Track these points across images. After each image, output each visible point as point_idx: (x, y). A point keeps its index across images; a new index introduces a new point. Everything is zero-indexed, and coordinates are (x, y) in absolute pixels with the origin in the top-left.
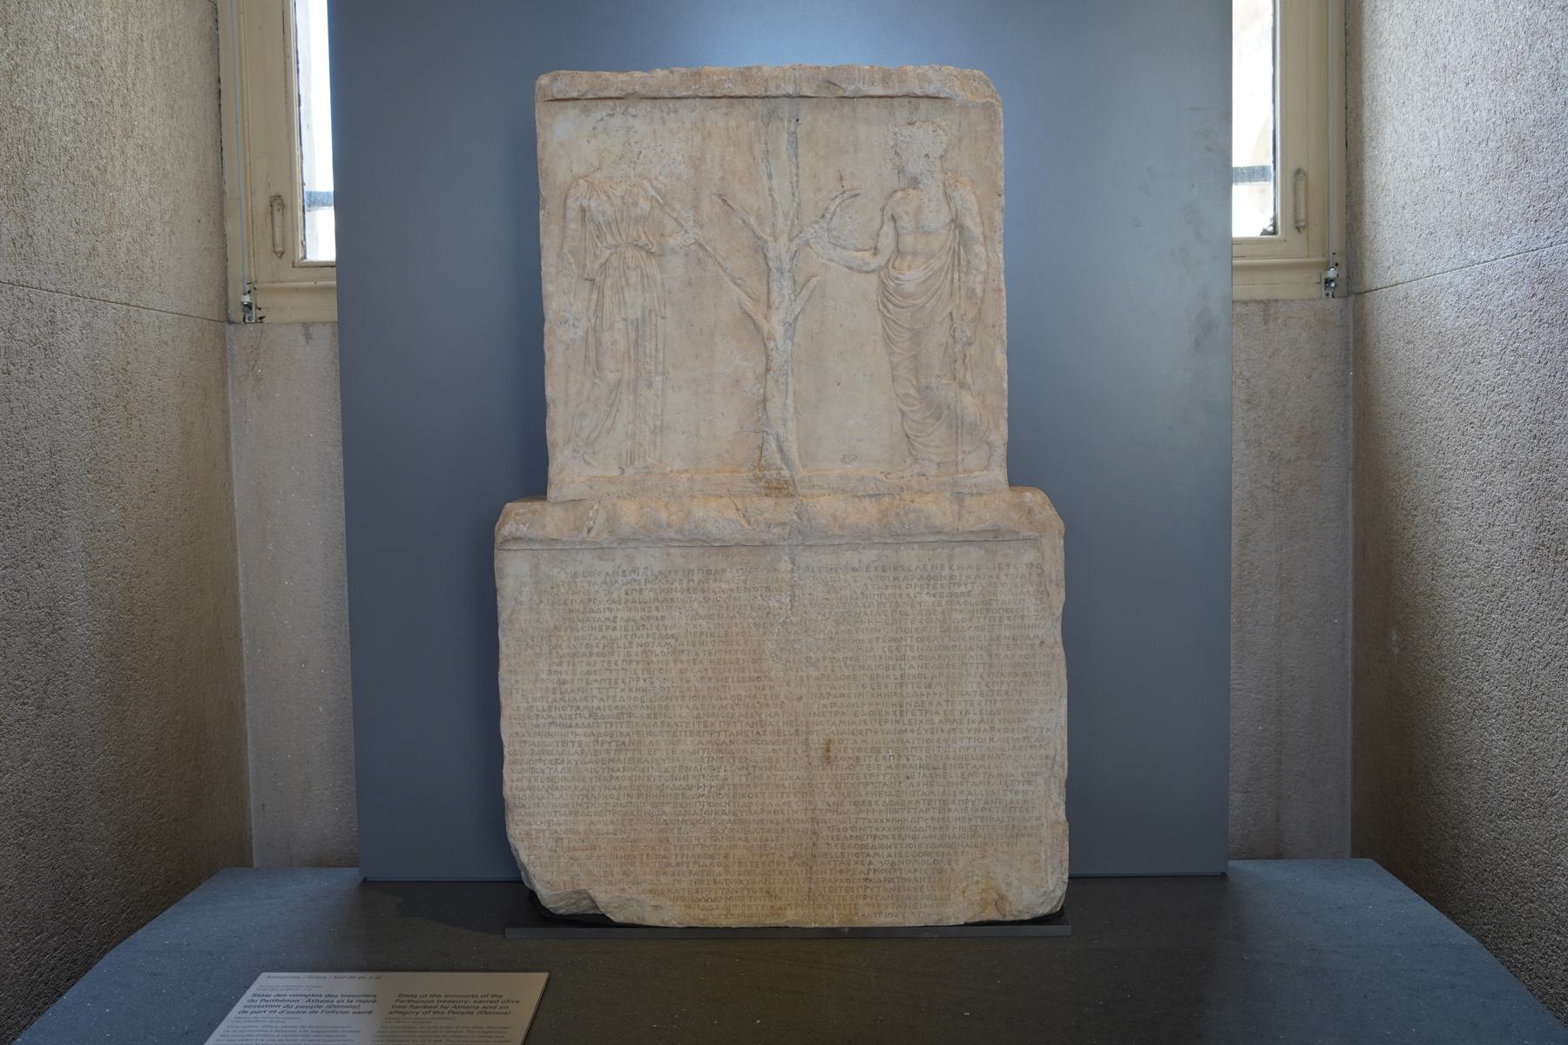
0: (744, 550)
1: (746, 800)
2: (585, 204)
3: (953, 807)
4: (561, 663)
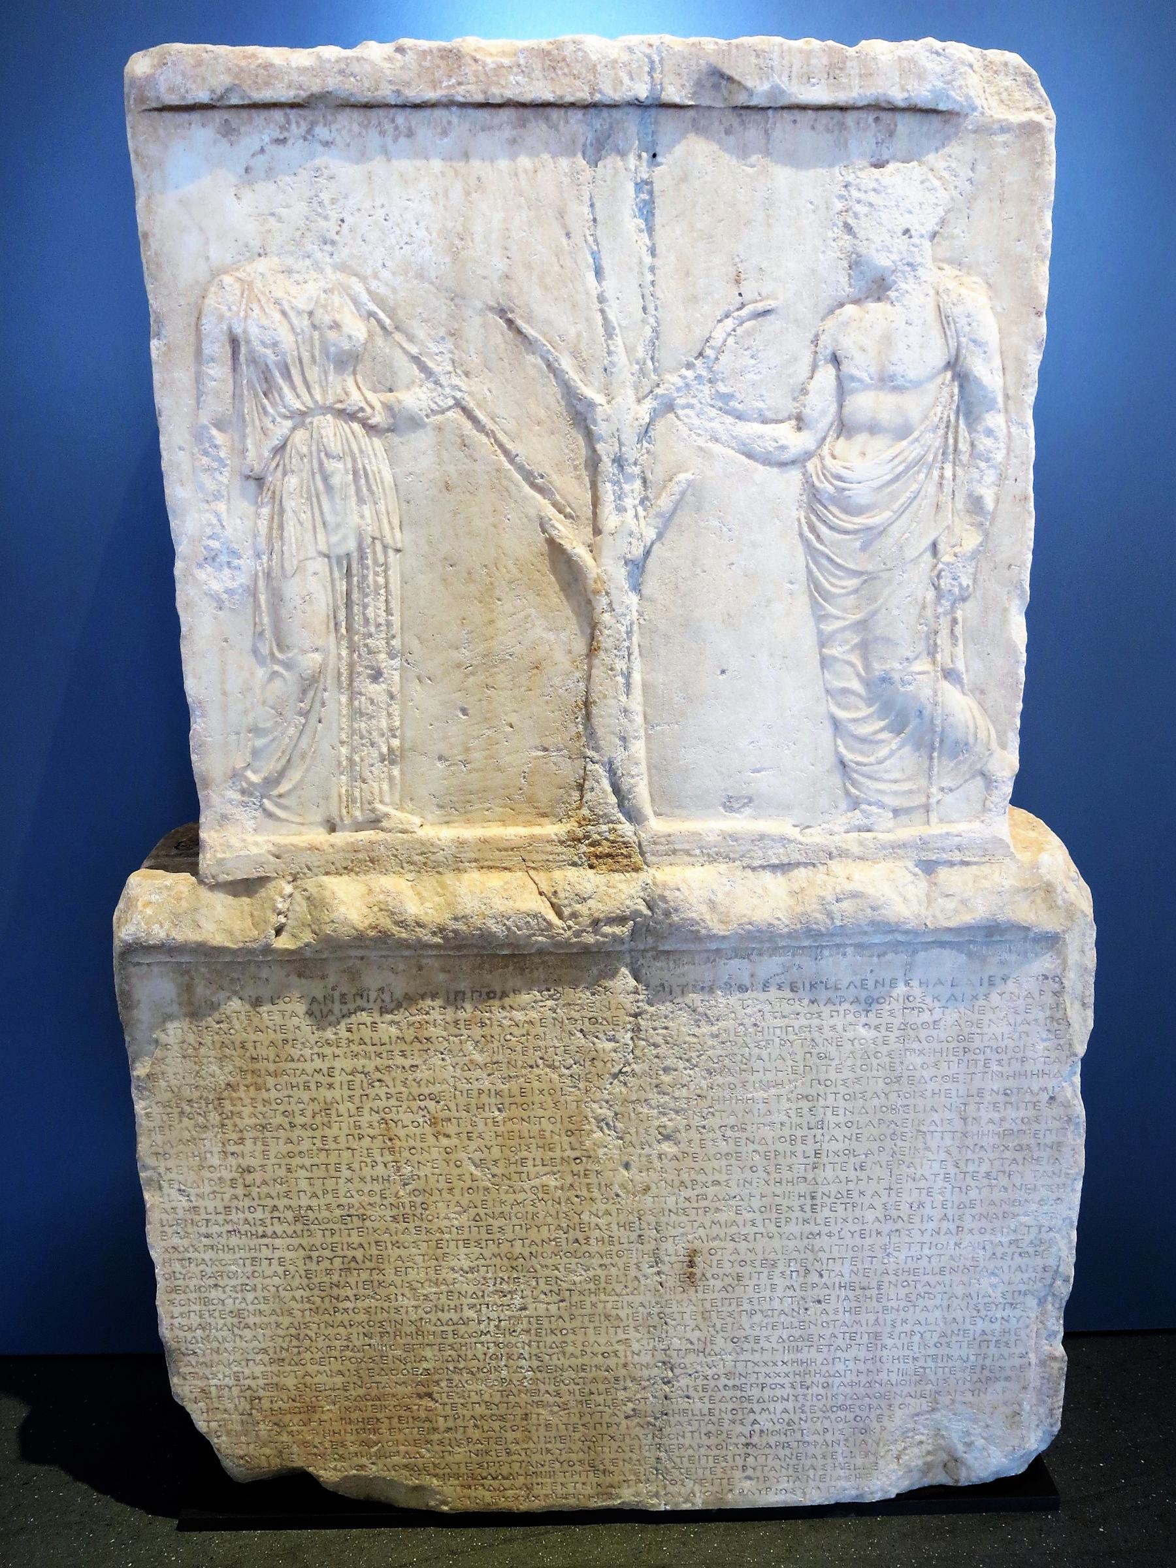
0: (550, 960)
1: (558, 1339)
2: (238, 330)
3: (889, 1342)
4: (242, 1140)
